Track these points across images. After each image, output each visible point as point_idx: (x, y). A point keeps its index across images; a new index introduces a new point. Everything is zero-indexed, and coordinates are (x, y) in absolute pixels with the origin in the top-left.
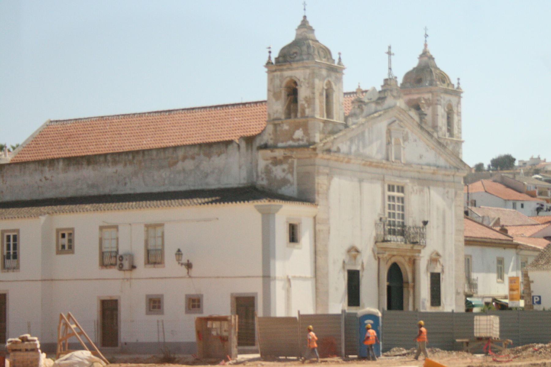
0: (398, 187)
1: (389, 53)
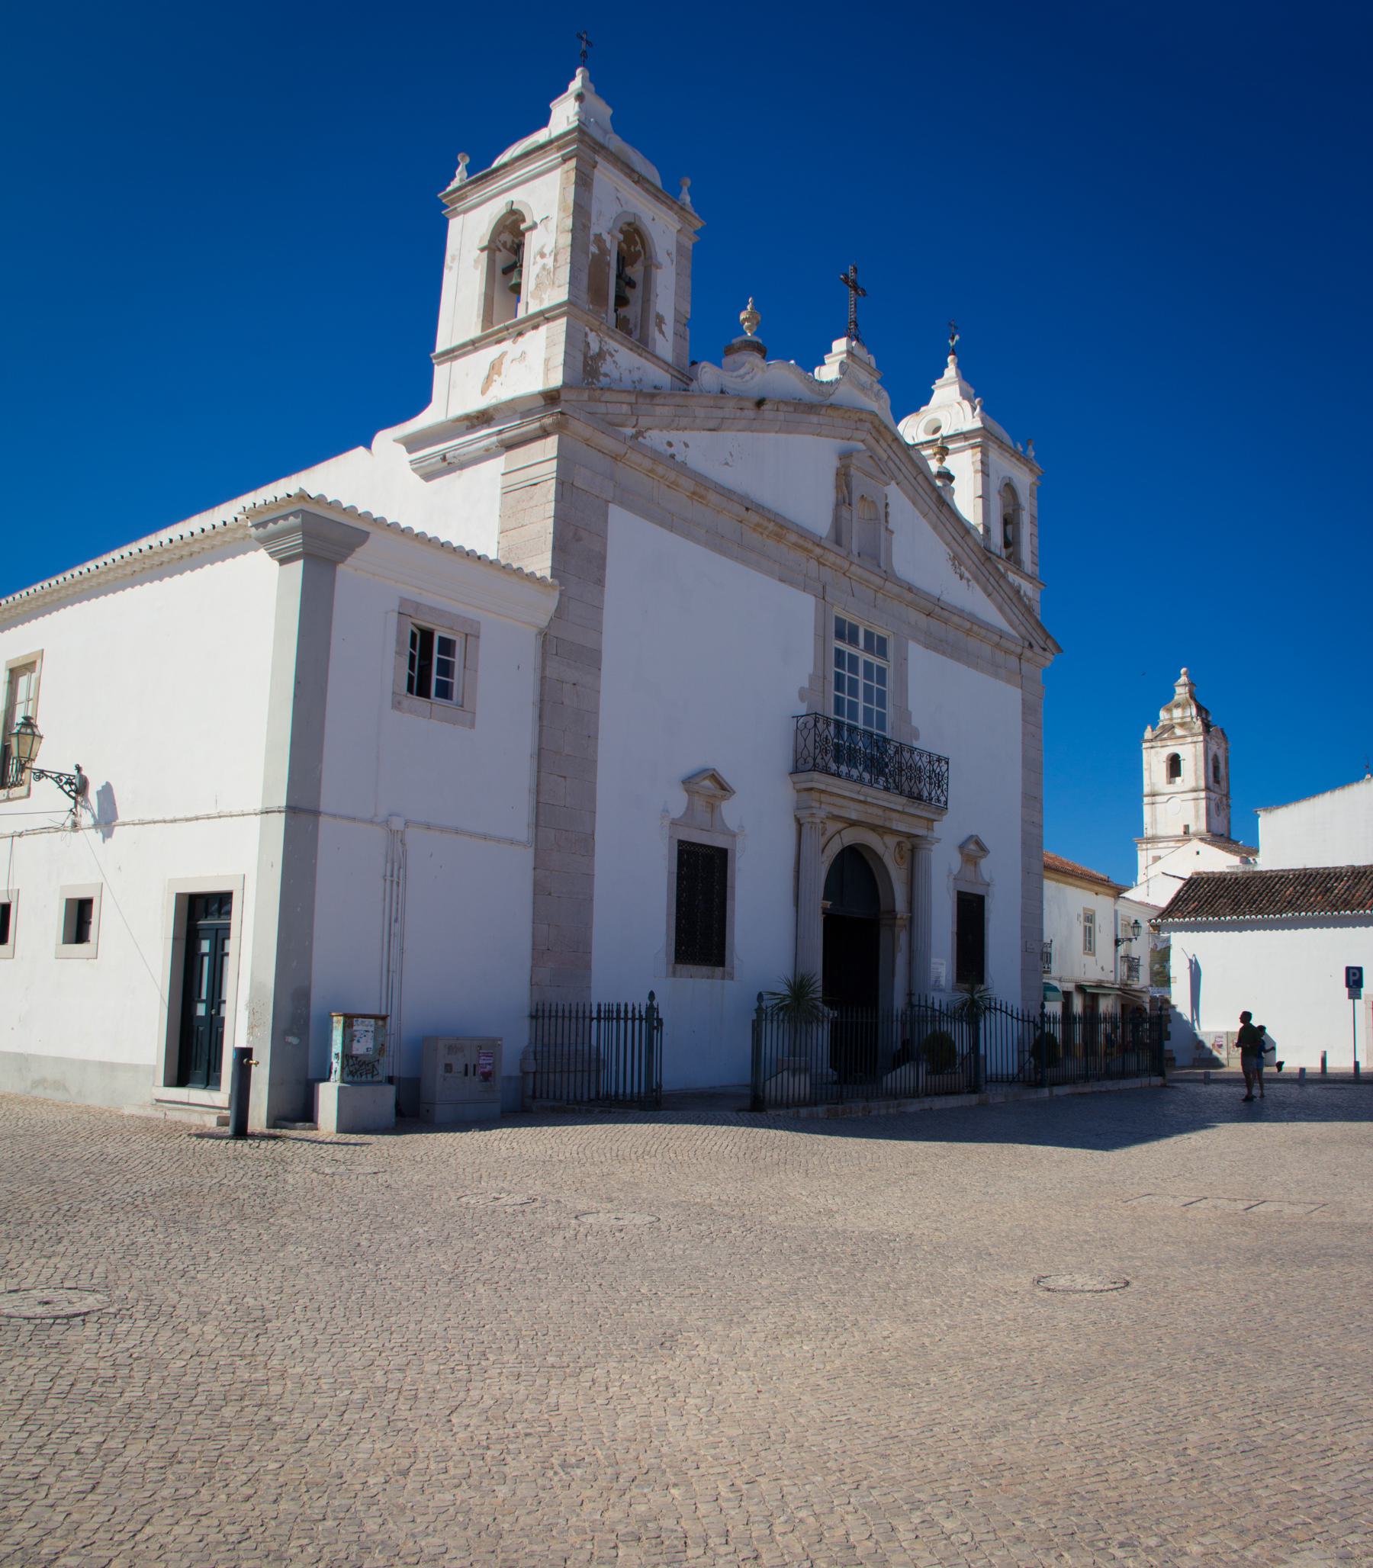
0: (869, 635)
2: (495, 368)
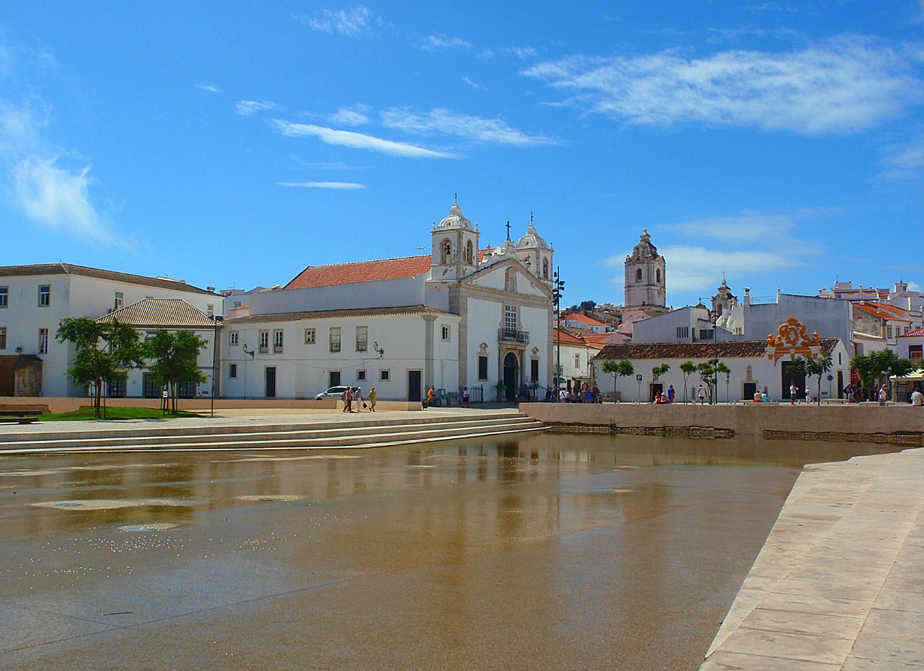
1: (508, 226)
2: (446, 271)
